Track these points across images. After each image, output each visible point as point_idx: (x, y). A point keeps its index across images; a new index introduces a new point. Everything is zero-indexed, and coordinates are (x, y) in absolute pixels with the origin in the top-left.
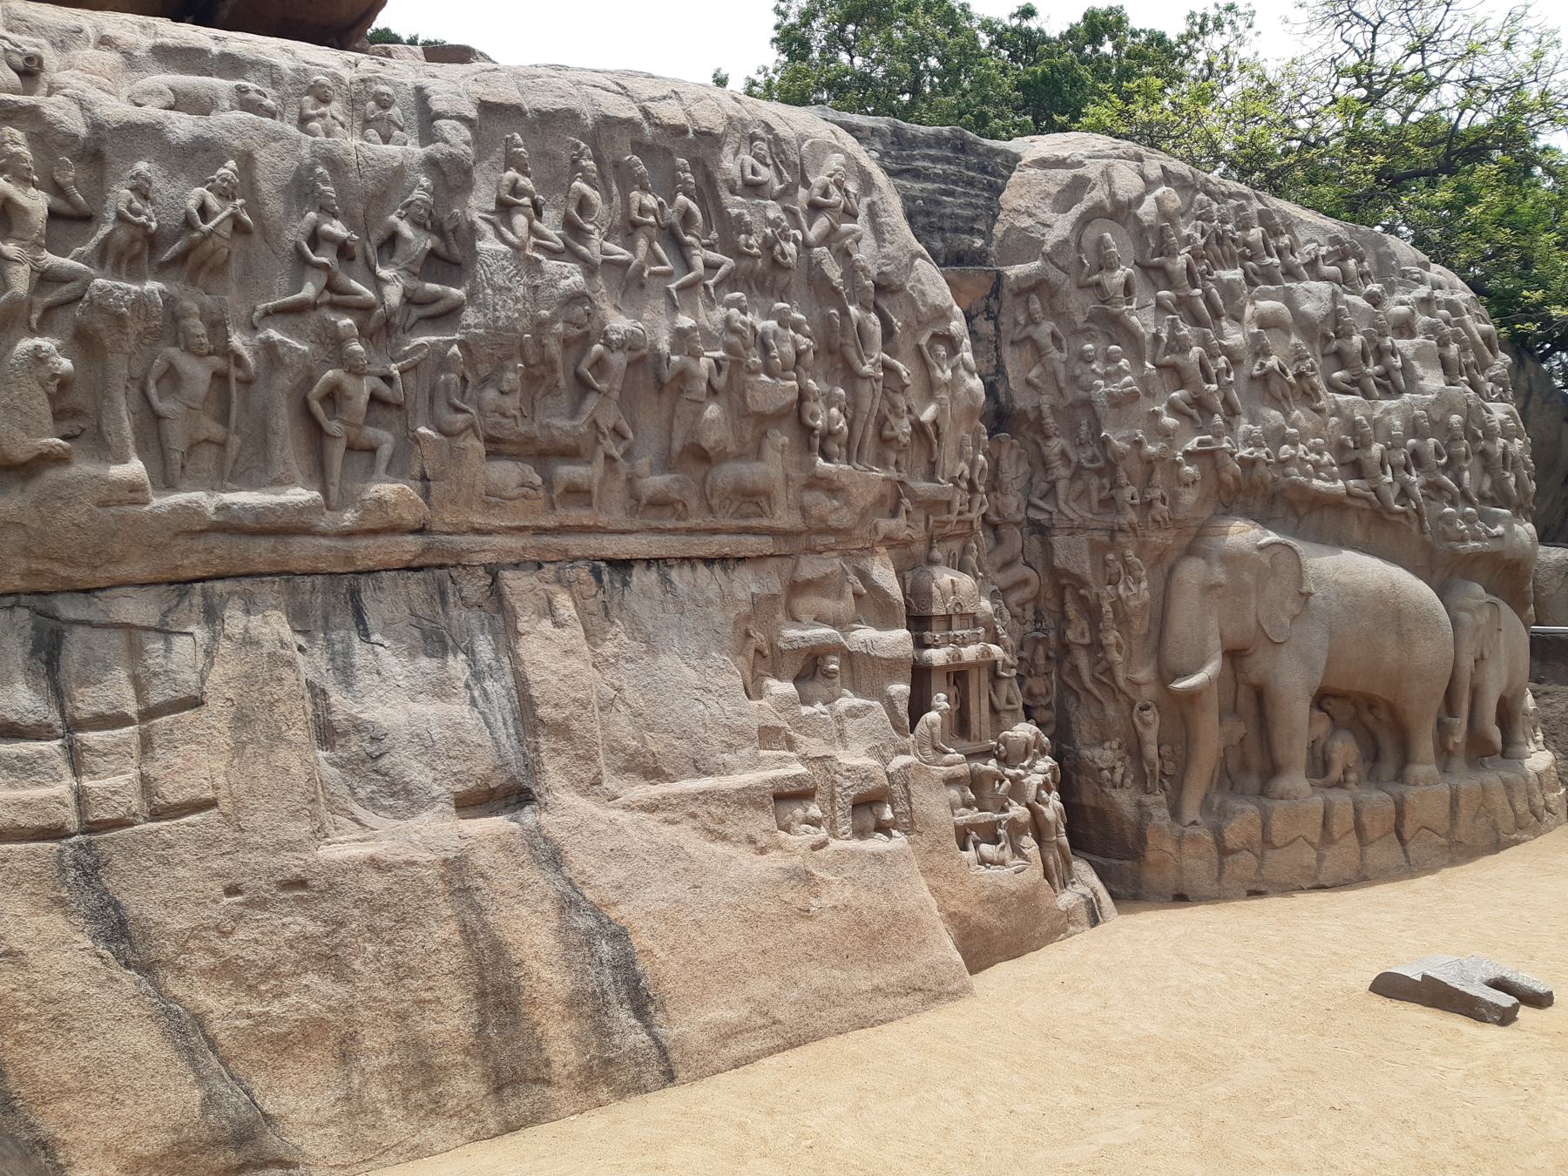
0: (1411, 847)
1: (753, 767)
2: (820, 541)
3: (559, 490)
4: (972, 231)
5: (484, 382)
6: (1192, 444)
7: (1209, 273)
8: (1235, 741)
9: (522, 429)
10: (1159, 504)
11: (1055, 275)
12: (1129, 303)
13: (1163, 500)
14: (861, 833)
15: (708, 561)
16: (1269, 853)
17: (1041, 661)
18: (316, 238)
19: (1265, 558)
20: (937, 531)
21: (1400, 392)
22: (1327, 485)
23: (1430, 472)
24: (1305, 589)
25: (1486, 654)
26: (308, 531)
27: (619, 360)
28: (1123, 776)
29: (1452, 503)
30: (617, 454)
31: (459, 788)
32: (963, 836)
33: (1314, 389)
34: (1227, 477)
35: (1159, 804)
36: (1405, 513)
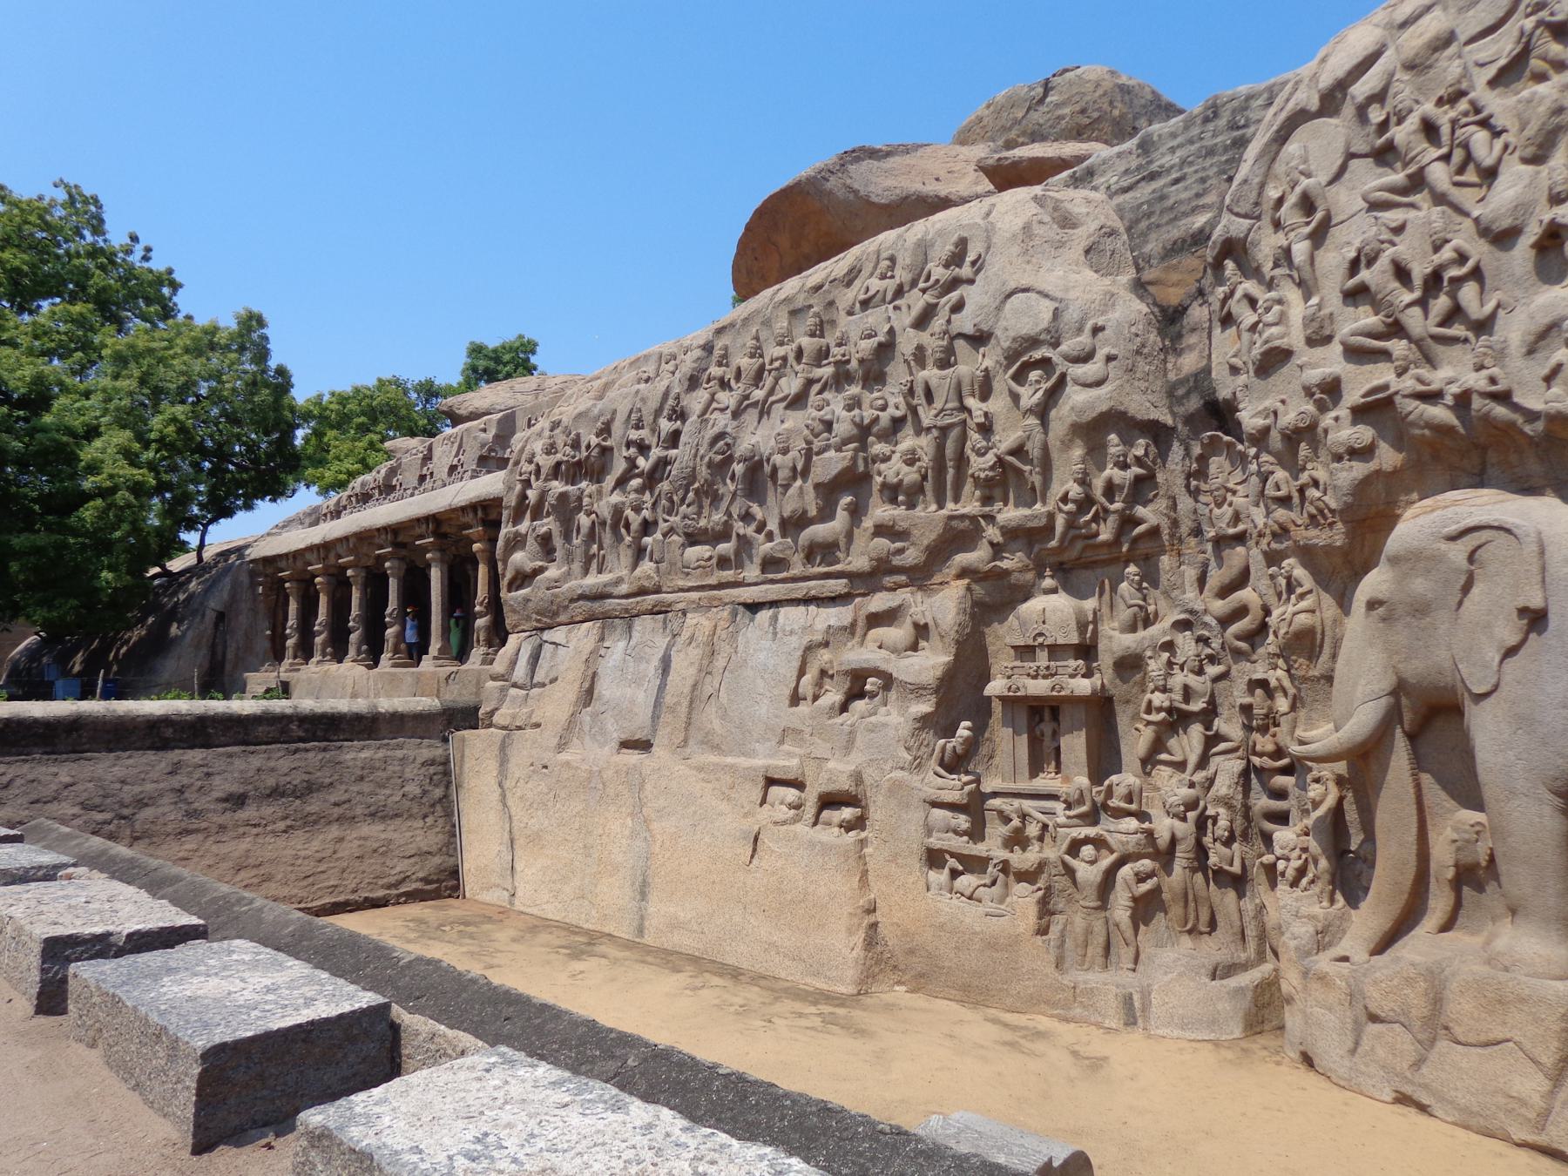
1: (770, 756)
2: (888, 580)
3: (714, 561)
4: (1193, 210)
5: (683, 500)
7: (1477, 111)
9: (702, 523)
11: (1236, 226)
12: (1308, 224)
14: (829, 824)
15: (807, 601)
16: (1443, 1045)
18: (629, 445)
19: (1457, 553)
20: (1052, 560)
26: (610, 596)
27: (739, 468)
28: (1301, 872)
30: (742, 532)
31: (624, 737)
32: (934, 858)
35: (1312, 917)
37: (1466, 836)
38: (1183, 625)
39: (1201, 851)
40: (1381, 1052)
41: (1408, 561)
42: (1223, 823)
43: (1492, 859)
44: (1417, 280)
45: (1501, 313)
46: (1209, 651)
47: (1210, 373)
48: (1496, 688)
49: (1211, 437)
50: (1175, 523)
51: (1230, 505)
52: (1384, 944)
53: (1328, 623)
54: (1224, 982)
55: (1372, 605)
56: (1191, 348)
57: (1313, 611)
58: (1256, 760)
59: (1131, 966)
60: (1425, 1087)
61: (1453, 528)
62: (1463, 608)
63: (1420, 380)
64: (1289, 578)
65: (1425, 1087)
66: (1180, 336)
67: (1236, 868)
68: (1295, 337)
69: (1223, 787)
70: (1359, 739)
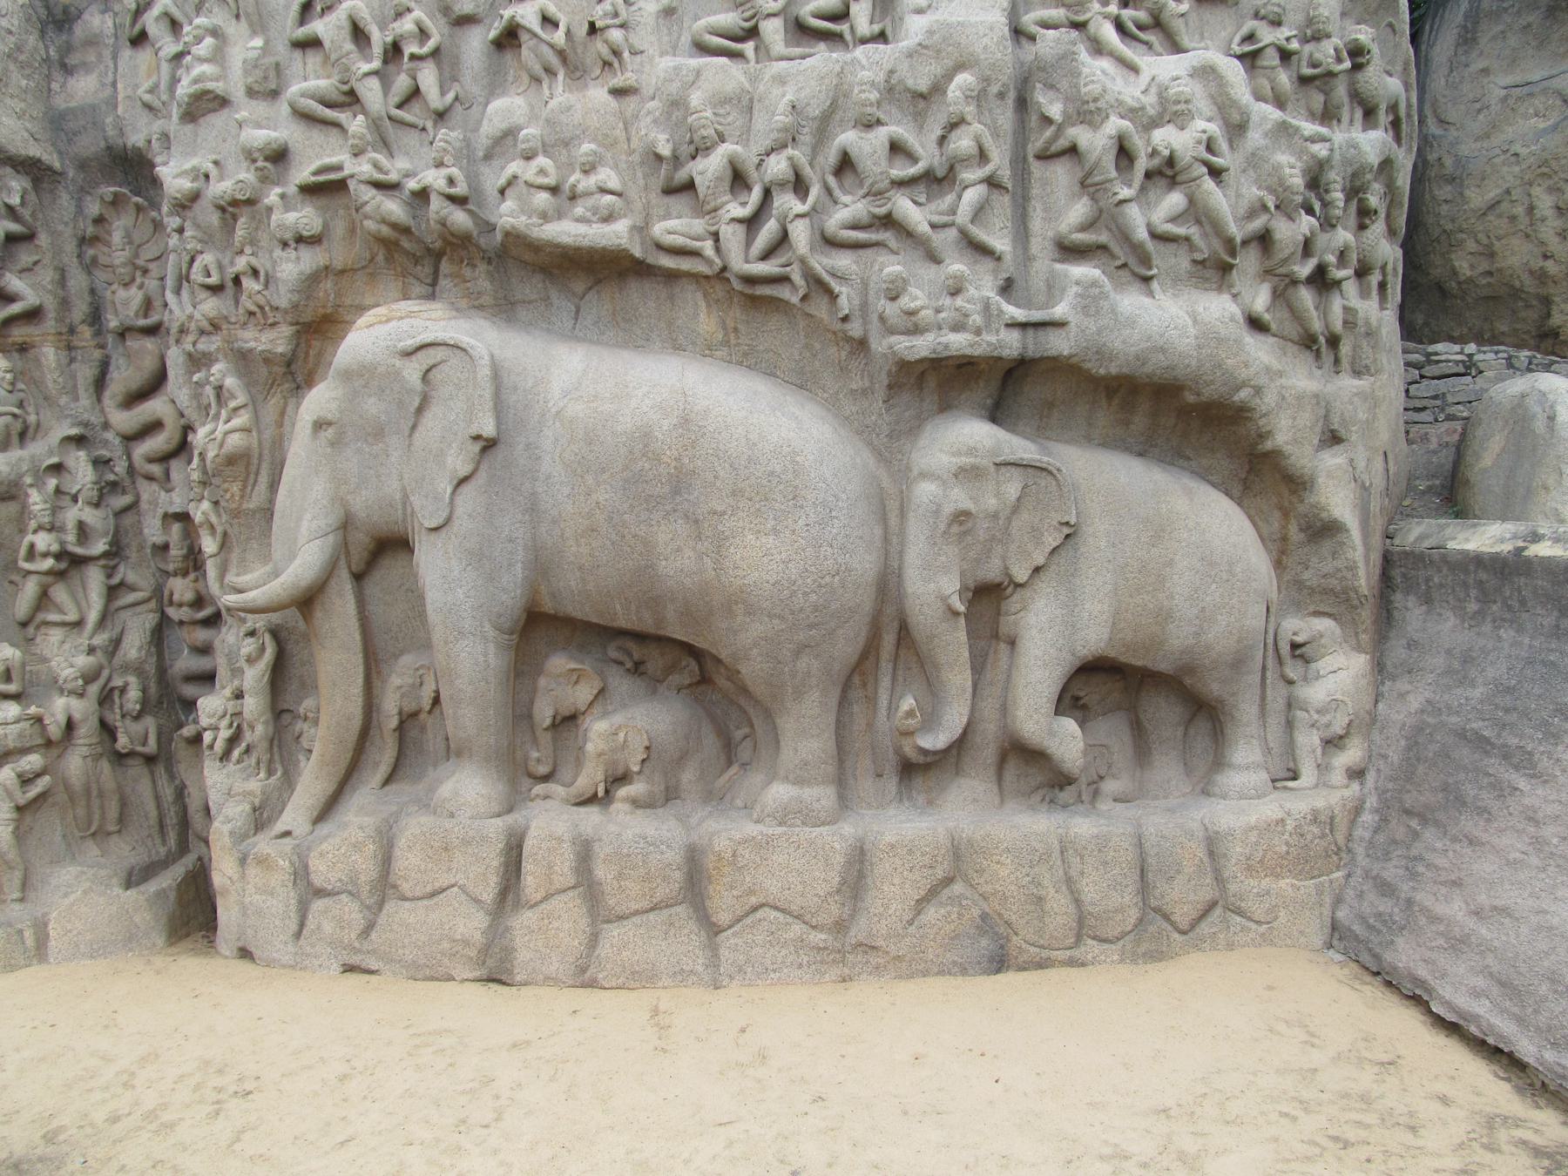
0: (727, 940)
6: (303, 173)
8: (426, 704)
10: (249, 284)
13: (255, 273)
17: (176, 552)
19: (412, 371)
21: (864, 41)
22: (582, 229)
23: (875, 194)
24: (474, 431)
25: (1021, 575)
28: (233, 741)
29: (934, 258)
33: (616, 53)
34: (370, 225)
35: (246, 794)
36: (783, 279)
37: (411, 681)
38: (80, 441)
39: (108, 730)
40: (328, 927)
41: (361, 376)
42: (134, 694)
43: (436, 701)
44: (377, 49)
45: (458, 108)
46: (112, 477)
47: (116, 107)
48: (448, 521)
49: (116, 194)
50: (65, 304)
51: (141, 287)
52: (327, 809)
53: (267, 445)
54: (142, 888)
55: (319, 425)
56: (86, 67)
57: (249, 431)
58: (172, 612)
59: (17, 895)
60: (374, 952)
61: (410, 343)
62: (417, 434)
63: (377, 166)
64: (219, 389)
65: (374, 952)
66: (68, 49)
67: (152, 746)
68: (234, 84)
69: (134, 647)
70: (304, 583)
